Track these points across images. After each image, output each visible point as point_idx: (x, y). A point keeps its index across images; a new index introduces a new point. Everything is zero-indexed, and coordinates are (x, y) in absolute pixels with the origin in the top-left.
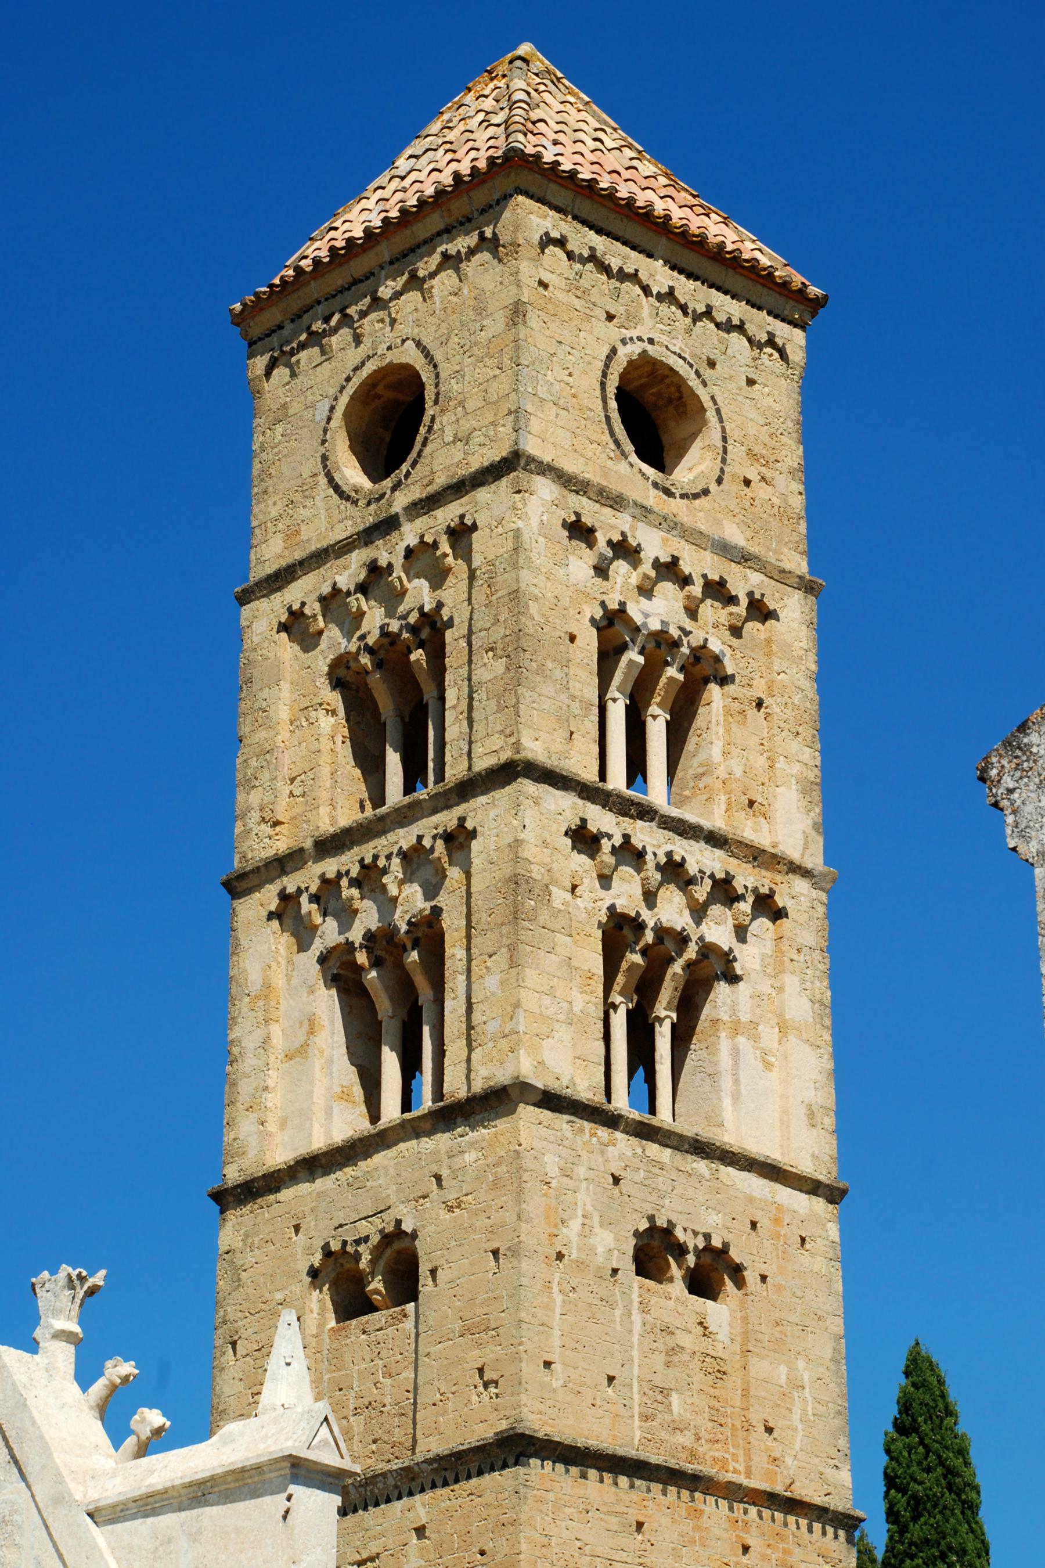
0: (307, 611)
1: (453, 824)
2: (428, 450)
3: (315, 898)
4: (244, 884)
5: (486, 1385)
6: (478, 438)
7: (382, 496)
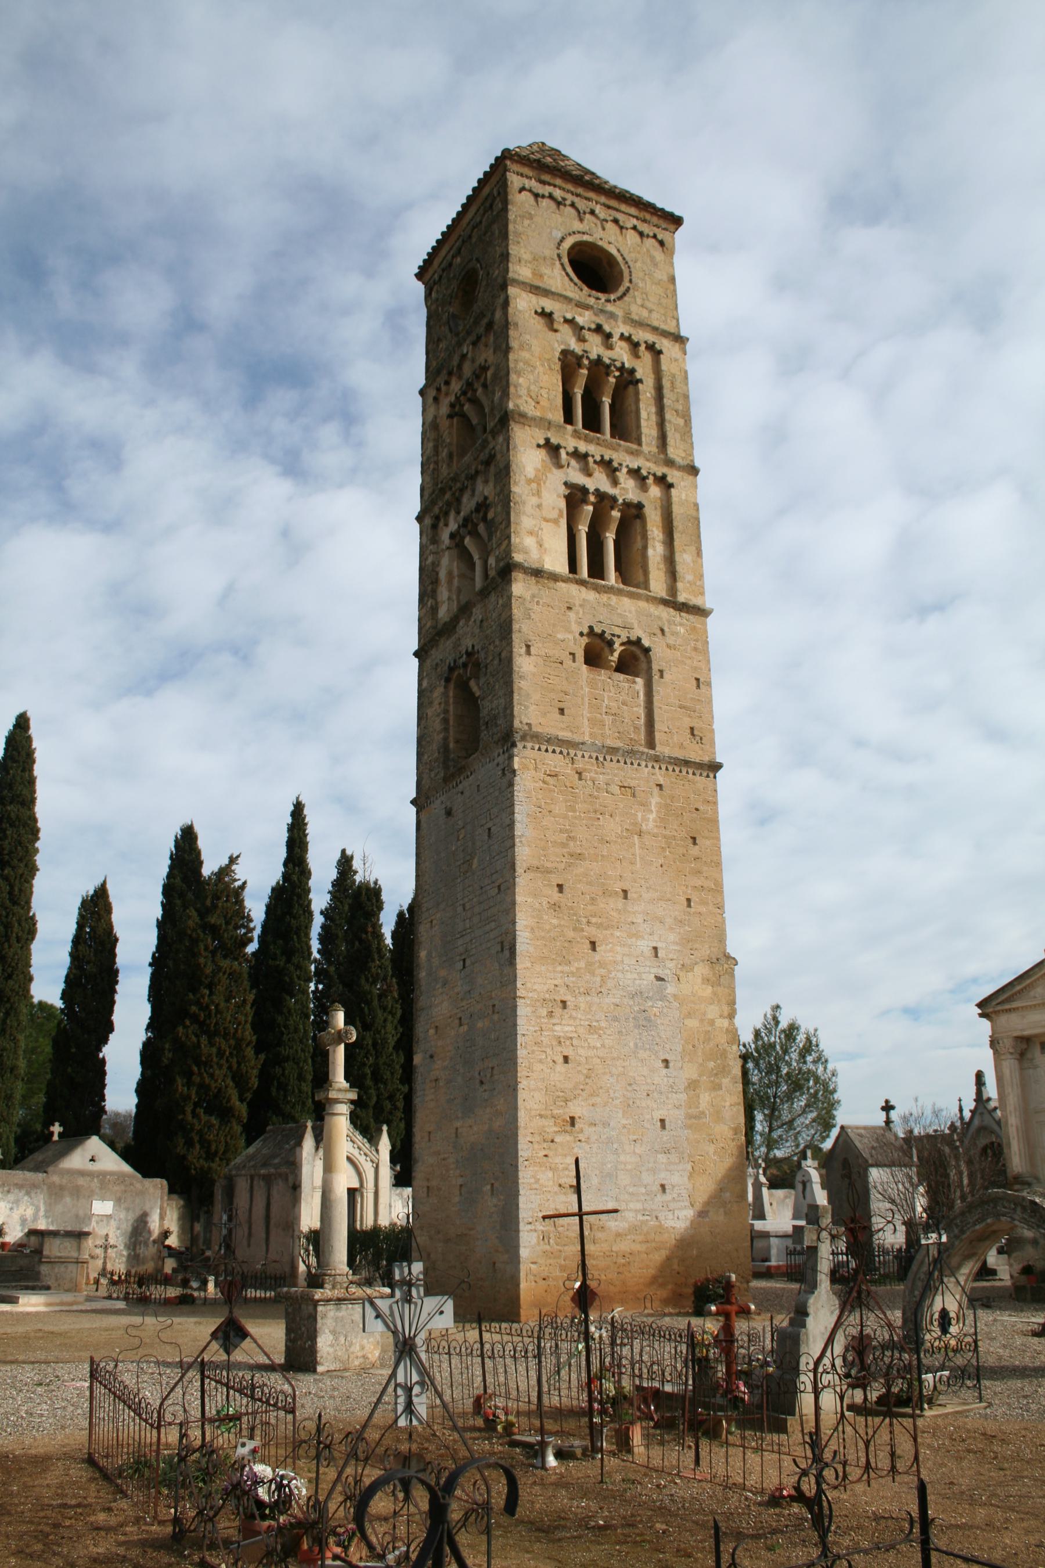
0: (555, 316)
1: (659, 474)
2: (626, 298)
3: (568, 454)
4: (522, 420)
5: (693, 734)
6: (654, 315)
7: (598, 299)
